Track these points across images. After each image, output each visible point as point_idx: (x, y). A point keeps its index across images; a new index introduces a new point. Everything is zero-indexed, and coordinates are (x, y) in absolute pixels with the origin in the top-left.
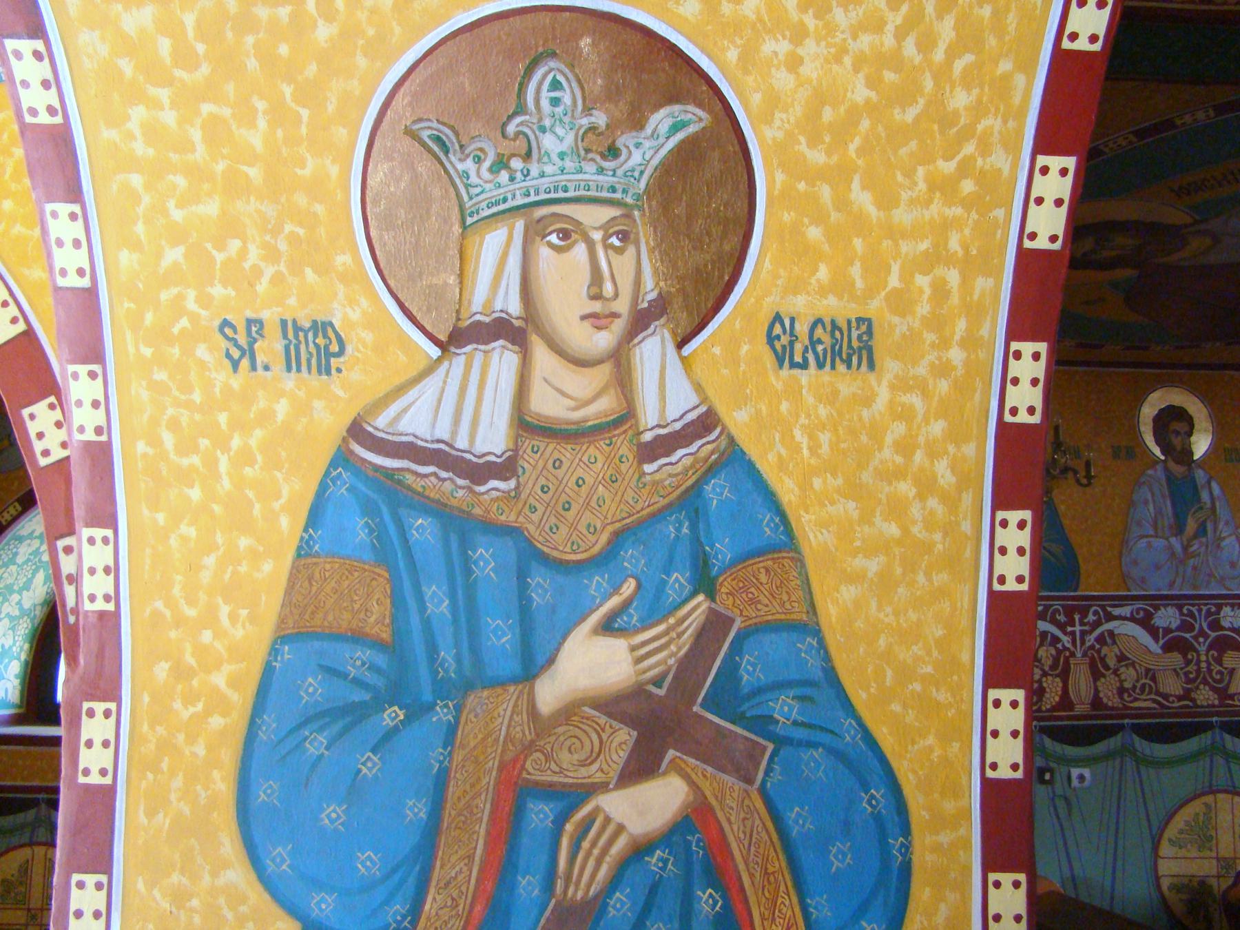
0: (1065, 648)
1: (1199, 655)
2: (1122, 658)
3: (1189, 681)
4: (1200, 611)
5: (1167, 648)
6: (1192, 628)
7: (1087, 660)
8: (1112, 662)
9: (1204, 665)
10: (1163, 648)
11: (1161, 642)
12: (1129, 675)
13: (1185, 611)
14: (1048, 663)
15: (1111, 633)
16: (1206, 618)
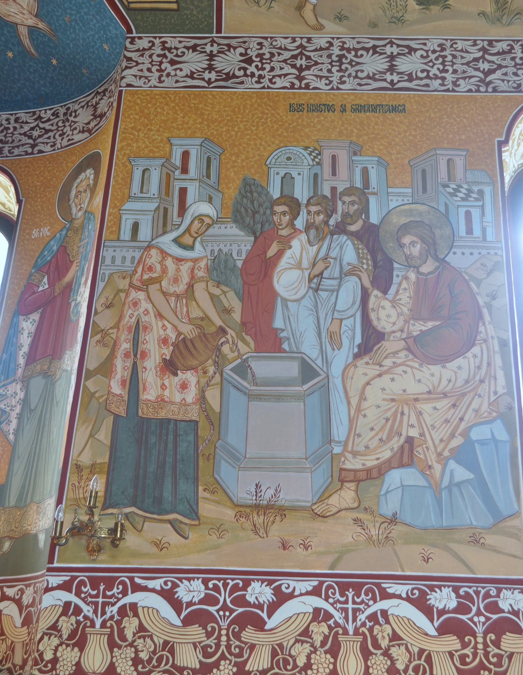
1: (220, 629)
2: (395, 637)
3: (207, 655)
5: (442, 630)
6: (216, 602)
11: (436, 624)
12: (400, 656)
13: (210, 585)
14: (318, 639)
15: (384, 613)
16: (483, 601)
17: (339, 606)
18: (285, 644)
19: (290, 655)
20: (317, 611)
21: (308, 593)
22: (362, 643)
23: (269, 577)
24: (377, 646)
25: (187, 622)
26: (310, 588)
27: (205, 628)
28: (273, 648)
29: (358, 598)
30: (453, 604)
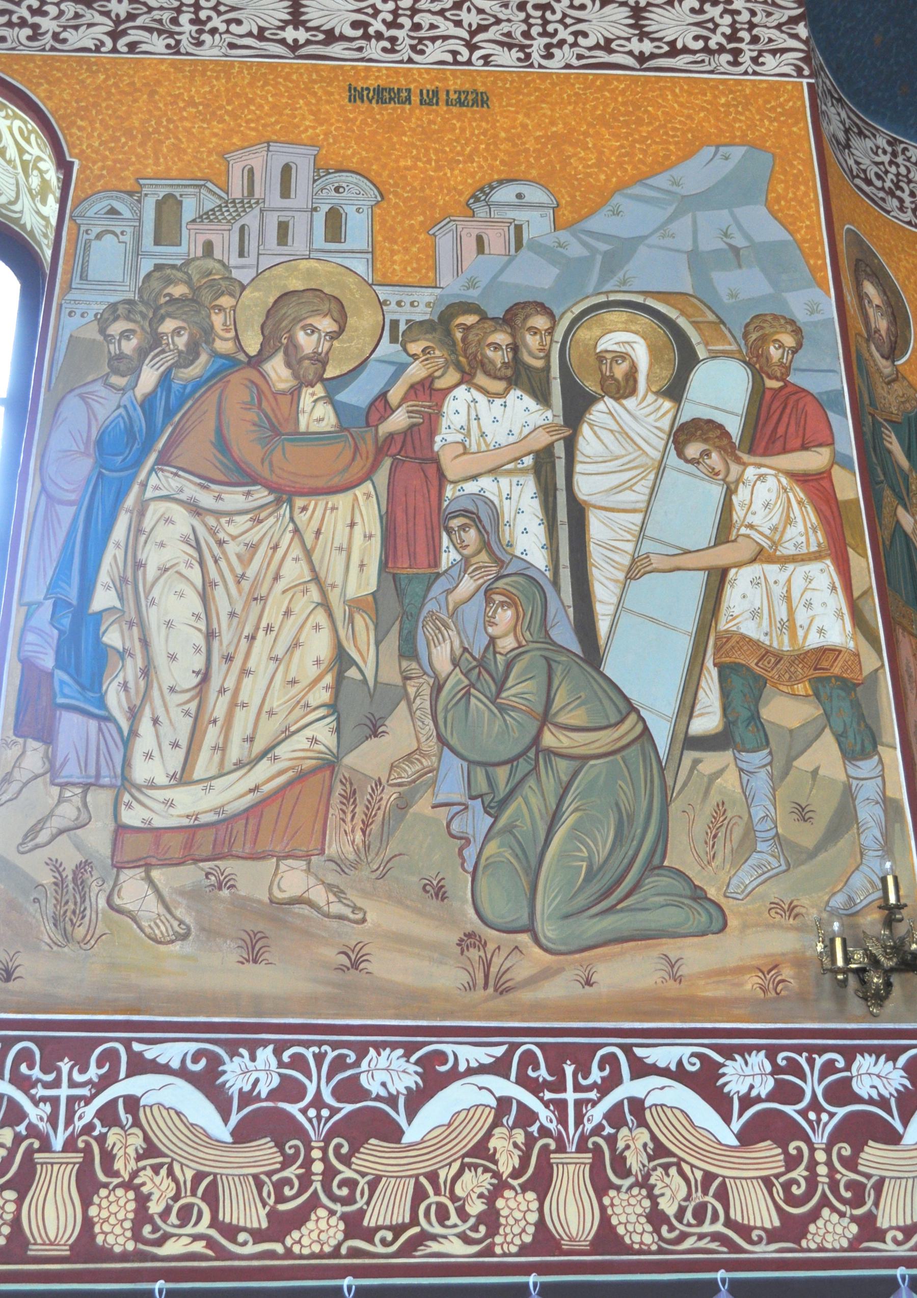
0: (544, 1132)
2: (659, 1150)
4: (811, 1062)
7: (587, 1157)
8: (634, 1160)
9: (822, 1170)
10: (738, 1136)
11: (736, 1125)
14: (507, 1163)
17: (548, 1095)
18: (442, 1174)
19: (454, 1198)
20: (504, 1103)
21: (483, 1069)
22: (592, 1166)
23: (406, 1040)
24: (623, 1170)
25: (243, 1134)
26: (488, 1060)
27: (280, 1146)
28: (418, 1185)
29: (585, 1078)
30: (765, 1087)
